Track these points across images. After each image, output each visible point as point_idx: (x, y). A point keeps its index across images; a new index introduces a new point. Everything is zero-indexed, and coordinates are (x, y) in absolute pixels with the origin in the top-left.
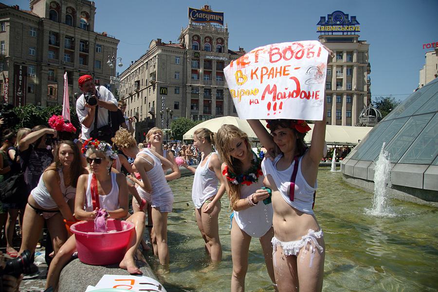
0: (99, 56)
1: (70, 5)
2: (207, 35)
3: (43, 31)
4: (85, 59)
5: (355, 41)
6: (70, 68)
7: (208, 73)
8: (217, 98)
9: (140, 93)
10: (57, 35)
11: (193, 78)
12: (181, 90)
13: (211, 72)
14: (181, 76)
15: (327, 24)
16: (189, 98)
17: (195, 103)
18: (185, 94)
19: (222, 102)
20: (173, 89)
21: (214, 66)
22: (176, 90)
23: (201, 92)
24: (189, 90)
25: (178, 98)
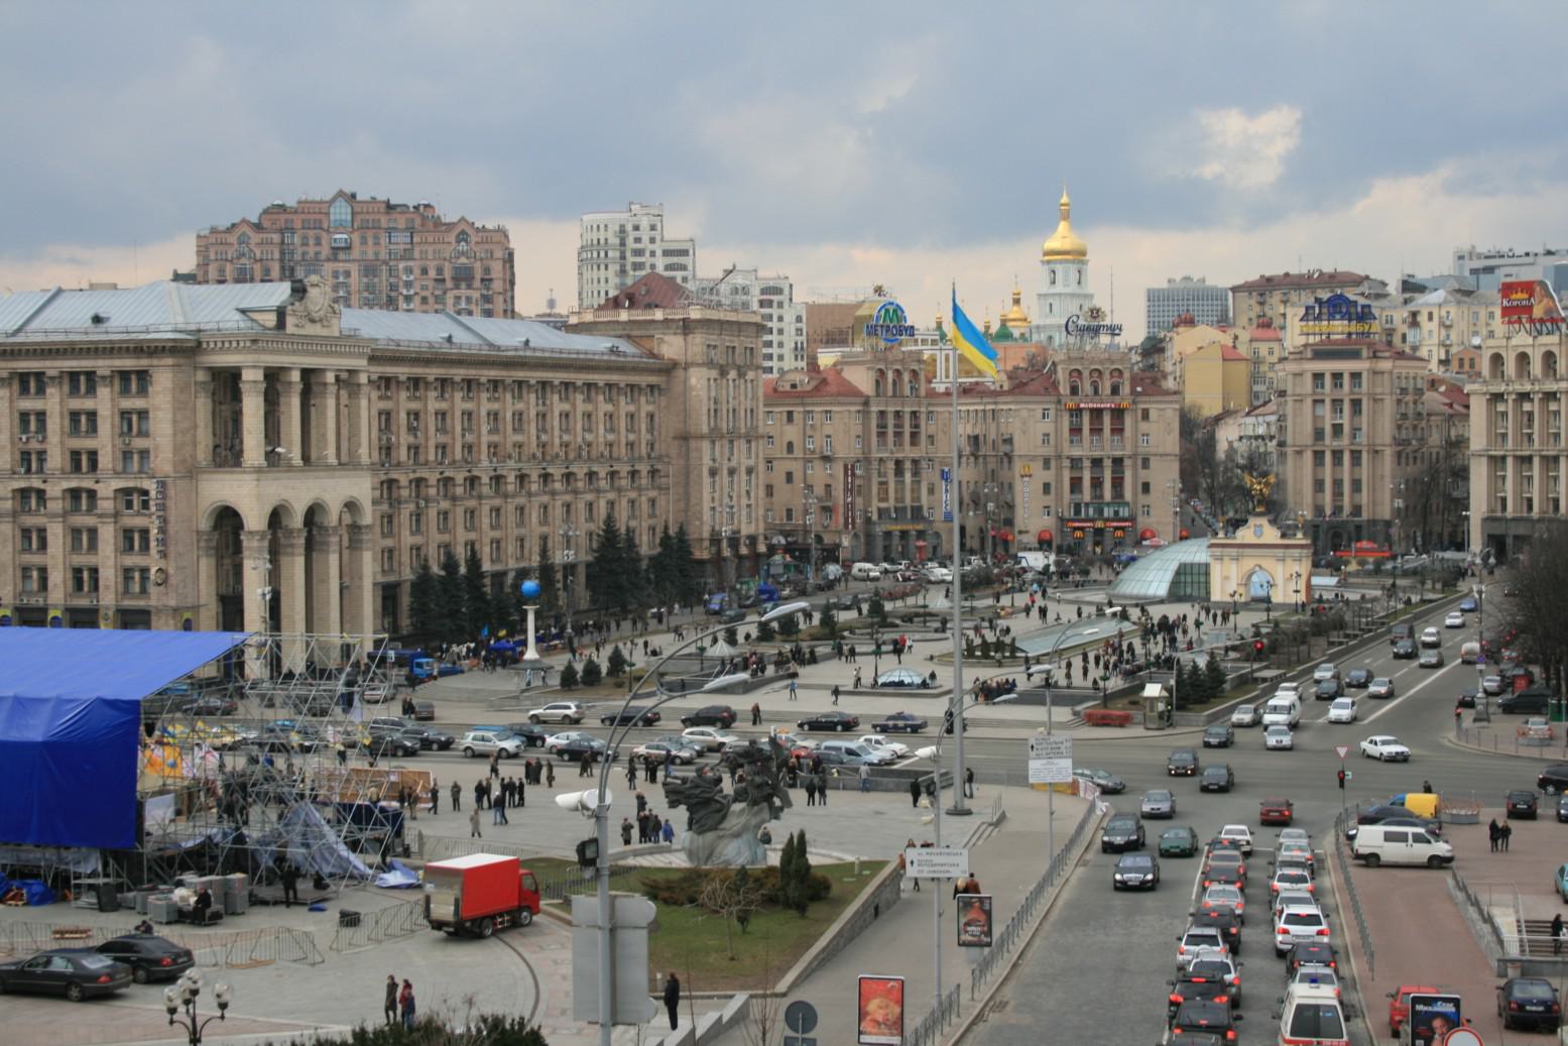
3: (869, 412)
4: (914, 436)
5: (1365, 353)
6: (900, 455)
7: (1096, 430)
8: (1113, 472)
9: (981, 460)
10: (882, 413)
11: (1072, 442)
12: (1053, 464)
13: (1101, 430)
15: (1318, 318)
16: (1067, 475)
17: (1076, 485)
18: (1060, 468)
19: (1122, 478)
20: (1041, 464)
21: (1107, 419)
22: (1047, 463)
23: (1087, 464)
24: (1067, 463)
25: (1049, 476)
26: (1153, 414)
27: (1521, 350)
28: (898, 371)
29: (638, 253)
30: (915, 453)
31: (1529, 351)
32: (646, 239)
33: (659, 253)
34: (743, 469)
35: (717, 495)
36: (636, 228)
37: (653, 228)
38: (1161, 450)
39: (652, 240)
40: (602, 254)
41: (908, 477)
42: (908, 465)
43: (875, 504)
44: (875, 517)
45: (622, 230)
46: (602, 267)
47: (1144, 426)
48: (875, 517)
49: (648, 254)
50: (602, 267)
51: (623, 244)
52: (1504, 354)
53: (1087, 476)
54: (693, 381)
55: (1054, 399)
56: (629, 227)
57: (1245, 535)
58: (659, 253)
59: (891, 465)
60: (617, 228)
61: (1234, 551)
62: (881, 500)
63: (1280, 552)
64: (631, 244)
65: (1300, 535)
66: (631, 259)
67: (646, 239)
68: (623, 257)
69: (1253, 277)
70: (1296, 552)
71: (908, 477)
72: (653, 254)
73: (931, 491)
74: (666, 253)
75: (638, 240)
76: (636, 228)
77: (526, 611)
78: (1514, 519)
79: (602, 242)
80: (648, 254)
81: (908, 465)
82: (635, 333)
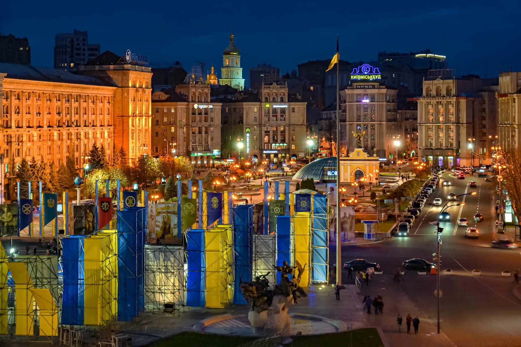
0: (212, 115)
1: (200, 90)
2: (274, 91)
6: (200, 125)
14: (258, 120)
16: (263, 132)
26: (296, 110)
27: (438, 85)
28: (200, 92)
29: (79, 49)
30: (206, 124)
31: (441, 86)
32: (81, 44)
33: (86, 49)
34: (144, 130)
35: (134, 141)
36: (78, 40)
37: (84, 40)
38: (299, 124)
39: (84, 45)
40: (64, 50)
41: (203, 133)
42: (204, 128)
43: (191, 144)
44: (191, 150)
45: (72, 41)
46: (64, 55)
47: (292, 114)
48: (191, 150)
49: (82, 50)
50: (64, 55)
51: (72, 46)
52: (431, 87)
53: (271, 134)
54: (126, 95)
55: (259, 103)
56: (75, 40)
57: (352, 155)
58: (86, 49)
59: (197, 129)
60: (70, 40)
61: (349, 162)
62: (193, 143)
63: (367, 162)
64: (75, 45)
65: (375, 155)
66: (75, 52)
67: (81, 44)
68: (72, 51)
69: (306, 62)
70: (374, 162)
71: (203, 133)
72: (84, 50)
73: (212, 139)
74: (89, 50)
75: (78, 44)
76: (78, 40)
77: (76, 191)
78: (436, 149)
79: (64, 45)
80: (82, 50)
81: (204, 128)
82: (102, 75)
